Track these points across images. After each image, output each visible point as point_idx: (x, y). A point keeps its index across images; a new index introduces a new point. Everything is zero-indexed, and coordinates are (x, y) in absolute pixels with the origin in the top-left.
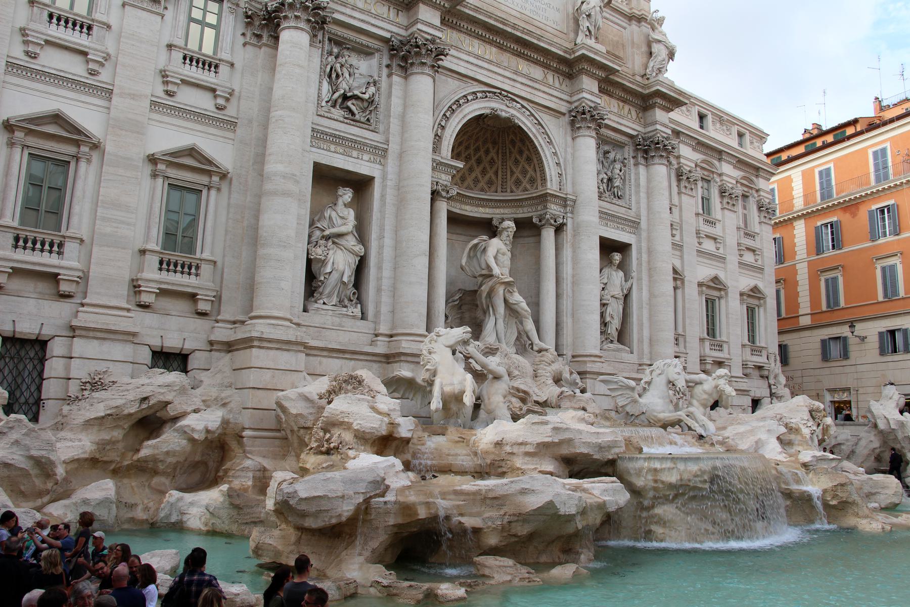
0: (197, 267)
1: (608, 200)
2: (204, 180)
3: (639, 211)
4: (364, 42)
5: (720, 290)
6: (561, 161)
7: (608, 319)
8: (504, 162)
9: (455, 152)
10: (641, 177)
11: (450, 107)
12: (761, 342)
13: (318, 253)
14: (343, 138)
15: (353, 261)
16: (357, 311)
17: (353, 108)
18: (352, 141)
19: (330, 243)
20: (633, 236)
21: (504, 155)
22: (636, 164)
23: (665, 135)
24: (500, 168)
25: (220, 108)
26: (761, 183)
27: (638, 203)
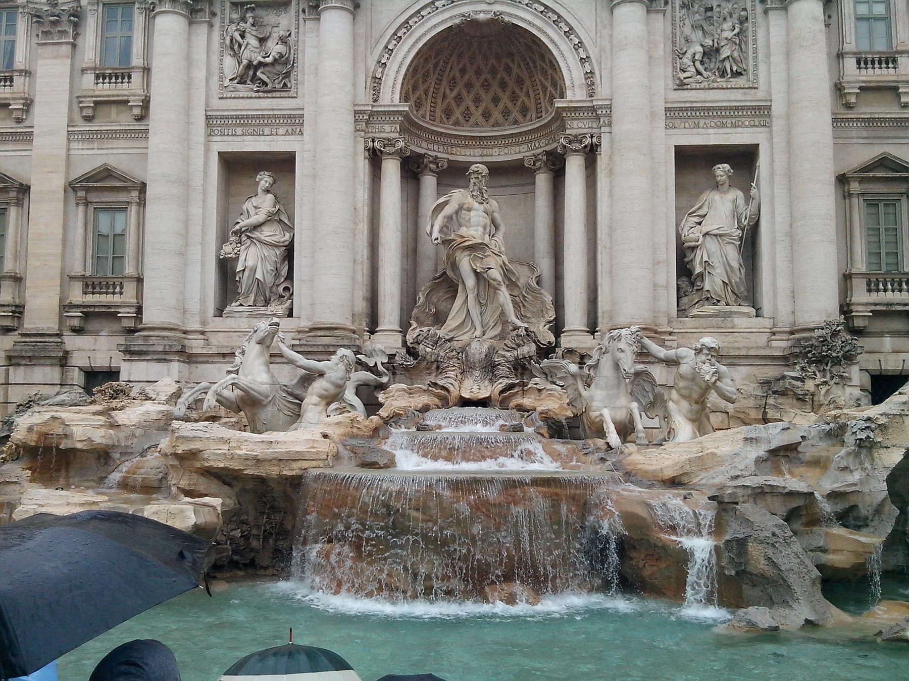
0: (122, 288)
2: (122, 197)
3: (770, 88)
6: (593, 53)
7: (698, 270)
9: (460, 86)
11: (395, 34)
14: (247, 117)
16: (281, 309)
17: (264, 77)
18: (258, 117)
19: (244, 238)
21: (528, 68)
22: (766, 12)
25: (140, 119)
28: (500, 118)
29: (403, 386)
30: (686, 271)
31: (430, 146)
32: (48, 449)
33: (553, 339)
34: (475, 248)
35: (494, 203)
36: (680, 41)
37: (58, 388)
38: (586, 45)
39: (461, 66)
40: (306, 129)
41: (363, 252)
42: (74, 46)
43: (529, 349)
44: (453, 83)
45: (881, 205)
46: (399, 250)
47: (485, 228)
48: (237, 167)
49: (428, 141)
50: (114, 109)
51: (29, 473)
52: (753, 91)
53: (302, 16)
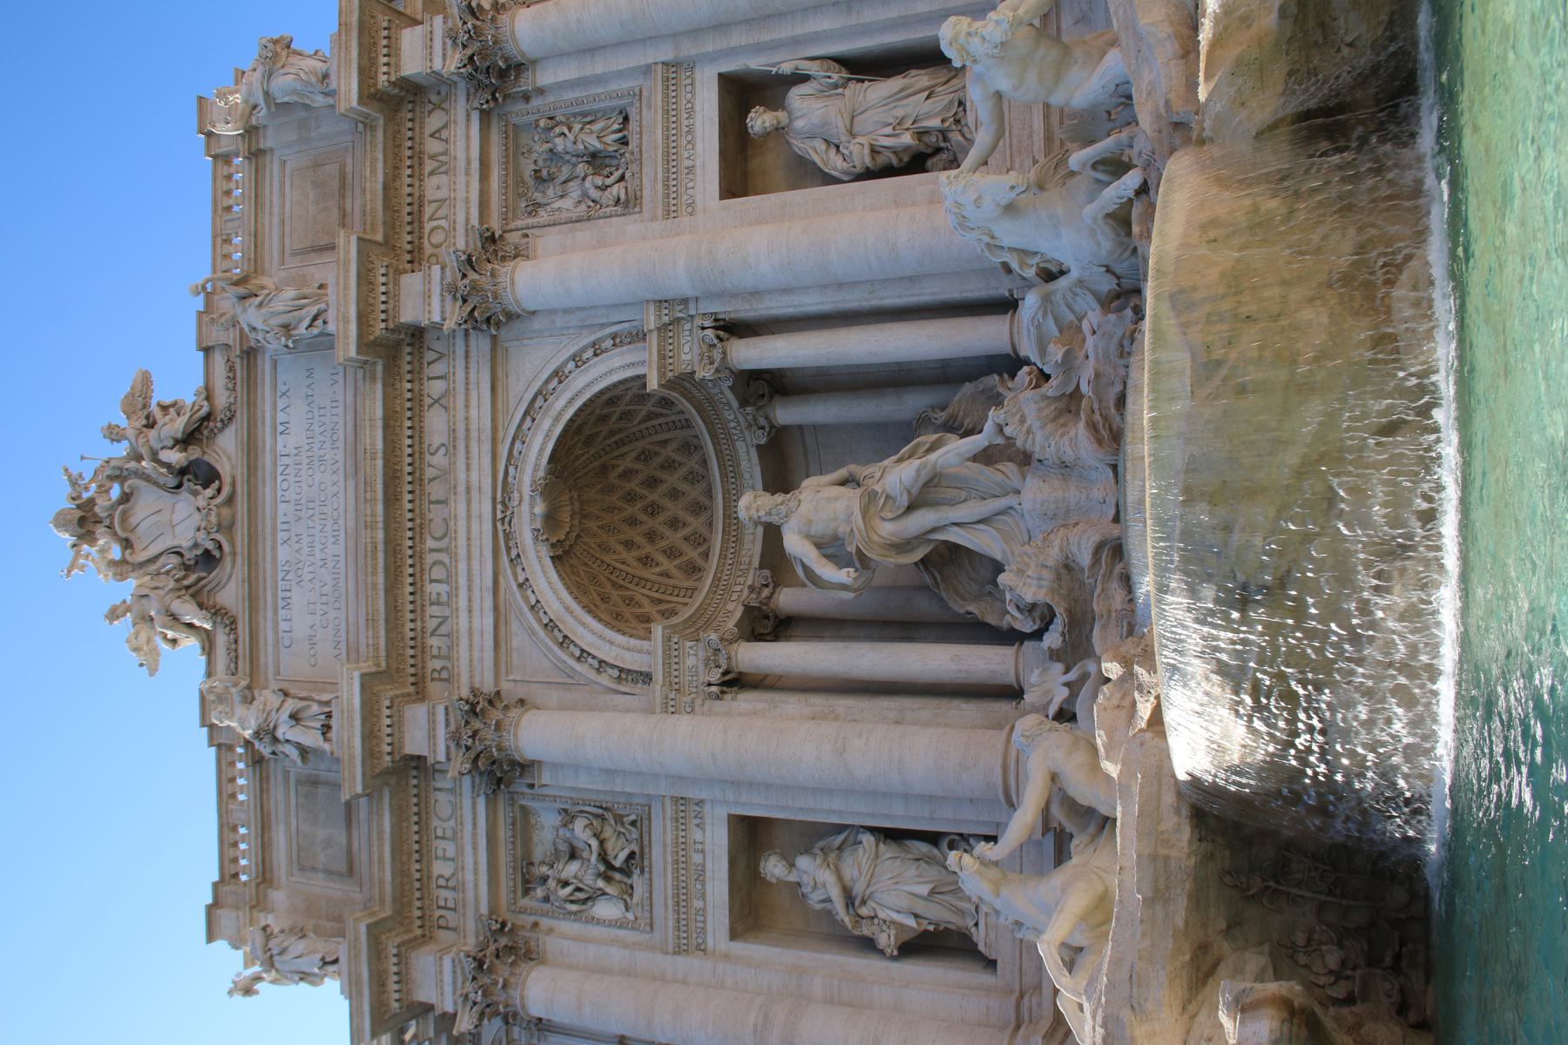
4: (510, 833)
7: (907, 139)
9: (648, 549)
10: (560, 79)
13: (886, 940)
17: (623, 856)
19: (864, 911)
20: (698, 75)
21: (620, 443)
23: (449, 42)
24: (649, 440)
27: (620, 74)
28: (701, 487)
30: (916, 163)
31: (735, 597)
33: (1026, 369)
35: (806, 483)
38: (576, 348)
39: (620, 548)
40: (692, 793)
44: (646, 561)
46: (881, 645)
52: (645, 93)
53: (537, 790)
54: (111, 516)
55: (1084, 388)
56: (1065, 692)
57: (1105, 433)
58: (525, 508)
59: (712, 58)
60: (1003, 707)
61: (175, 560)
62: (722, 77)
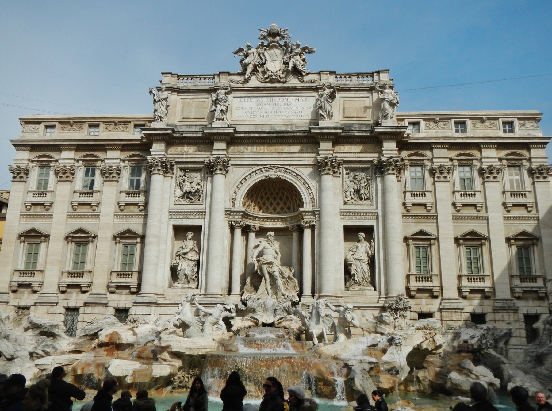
0: (132, 275)
1: (354, 203)
5: (480, 240)
6: (314, 191)
7: (353, 272)
8: (291, 196)
9: (265, 199)
12: (536, 270)
13: (175, 262)
14: (184, 212)
15: (192, 264)
16: (195, 285)
18: (188, 212)
26: (534, 152)
28: (280, 211)
29: (240, 318)
32: (112, 344)
33: (297, 299)
34: (270, 263)
36: (345, 187)
37: (104, 316)
41: (227, 264)
42: (118, 182)
43: (288, 304)
44: (262, 198)
45: (421, 248)
47: (273, 255)
48: (180, 231)
49: (252, 220)
50: (132, 207)
51: (106, 353)
53: (206, 176)
54: (275, 42)
55: (291, 316)
56: (229, 309)
57: (280, 321)
58: (274, 173)
59: (378, 224)
60: (226, 292)
61: (264, 61)
62: (374, 226)
